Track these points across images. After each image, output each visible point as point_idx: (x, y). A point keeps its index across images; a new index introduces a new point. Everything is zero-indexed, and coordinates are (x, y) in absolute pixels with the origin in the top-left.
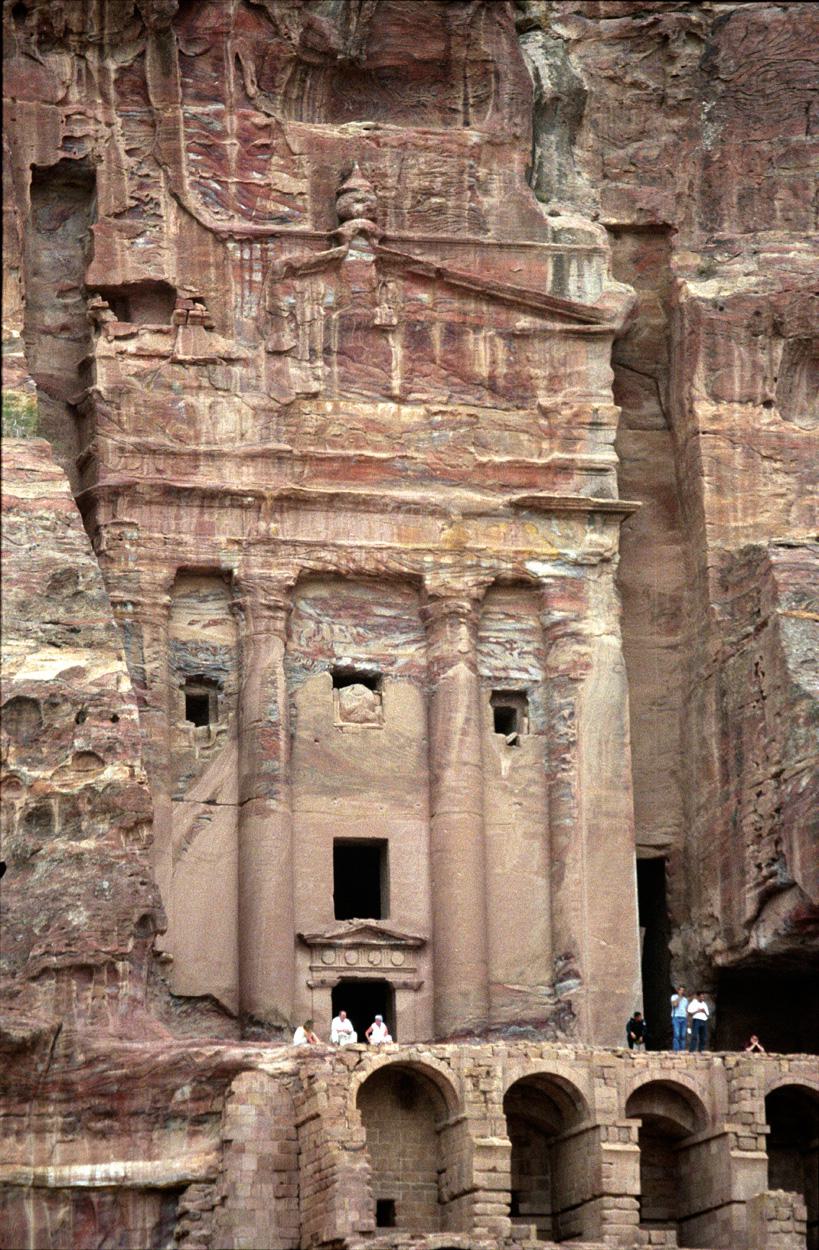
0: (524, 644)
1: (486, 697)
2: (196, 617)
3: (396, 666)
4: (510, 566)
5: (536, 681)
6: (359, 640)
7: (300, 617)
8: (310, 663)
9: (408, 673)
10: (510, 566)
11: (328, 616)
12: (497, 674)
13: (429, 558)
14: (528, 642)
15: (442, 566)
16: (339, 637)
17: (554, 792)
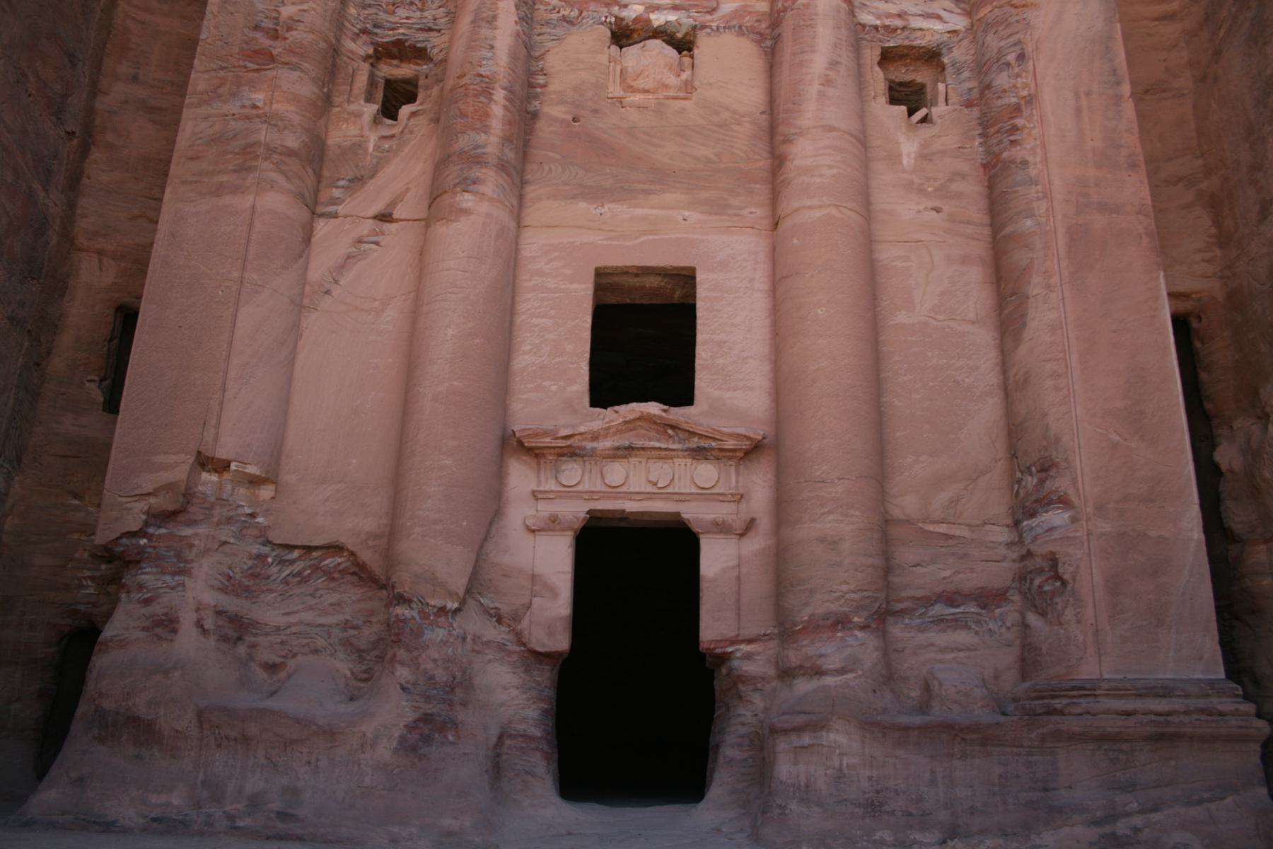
1: (871, 55)
3: (717, 15)
5: (954, 32)
8: (575, 13)
12: (887, 22)
17: (997, 177)
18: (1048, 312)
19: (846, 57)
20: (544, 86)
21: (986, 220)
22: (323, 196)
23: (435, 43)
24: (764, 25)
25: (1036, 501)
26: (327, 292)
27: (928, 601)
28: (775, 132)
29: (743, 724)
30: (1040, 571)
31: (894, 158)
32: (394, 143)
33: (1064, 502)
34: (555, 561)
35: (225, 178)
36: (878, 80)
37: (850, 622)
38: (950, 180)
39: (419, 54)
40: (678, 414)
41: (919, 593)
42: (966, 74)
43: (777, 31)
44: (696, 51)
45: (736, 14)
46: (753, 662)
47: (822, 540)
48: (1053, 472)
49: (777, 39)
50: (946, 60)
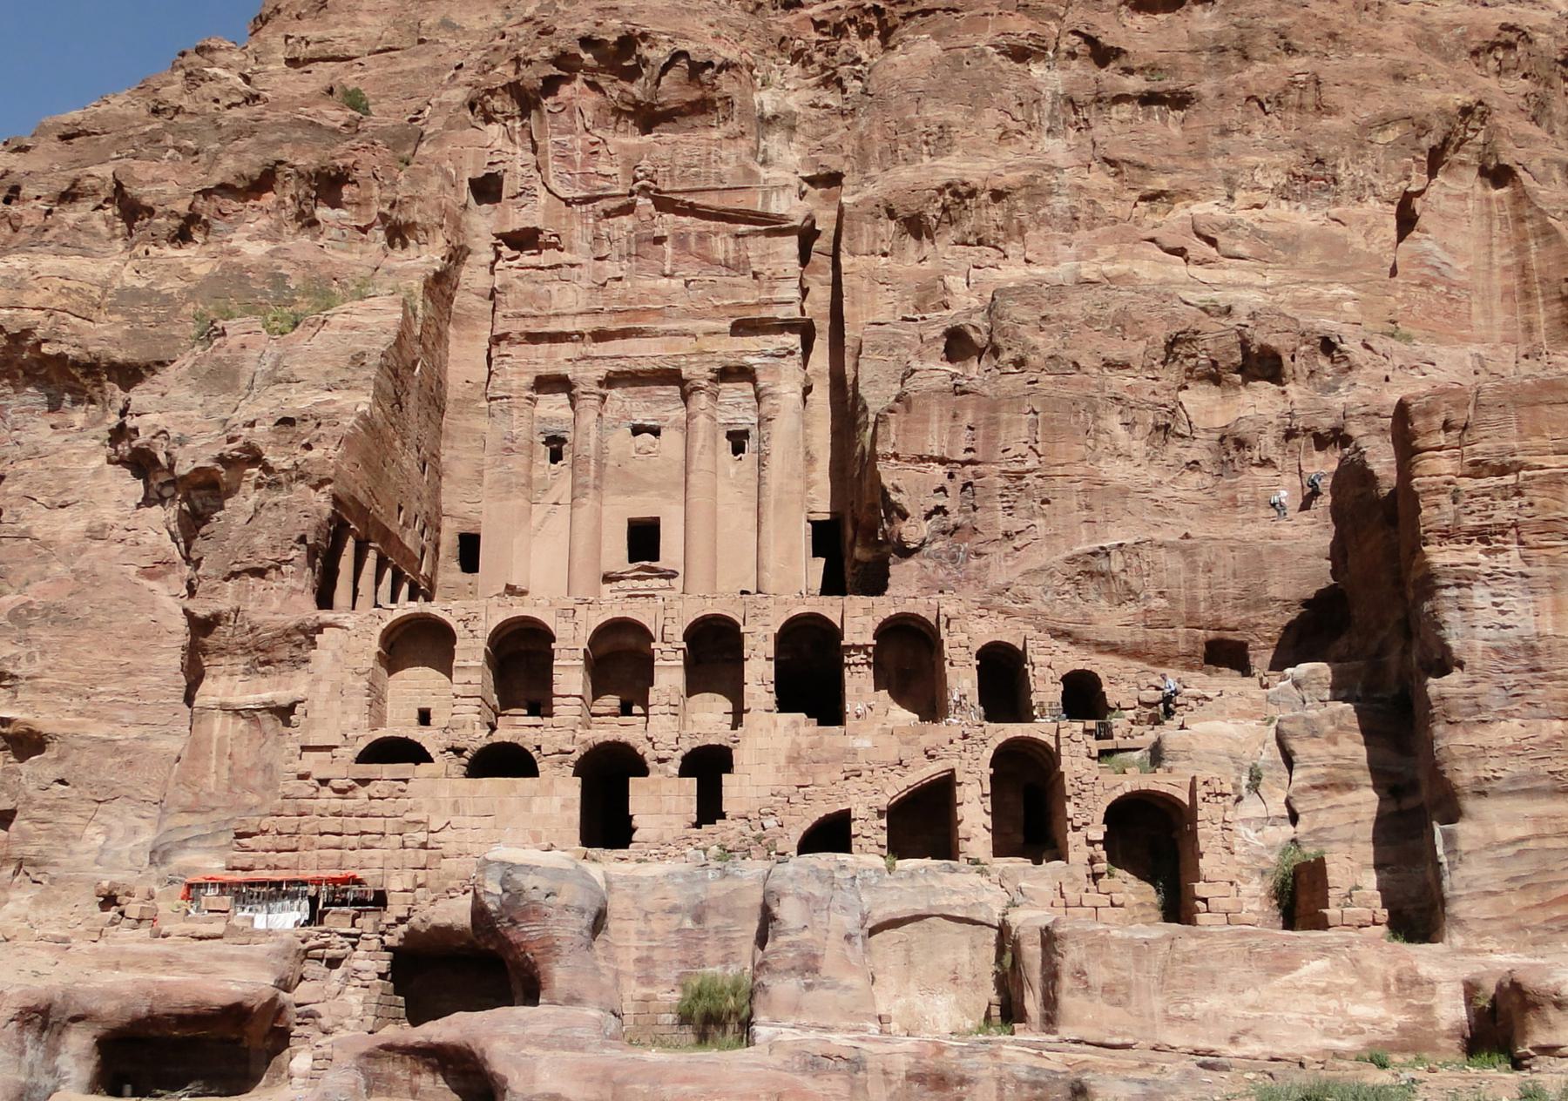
6: (647, 409)
9: (675, 426)
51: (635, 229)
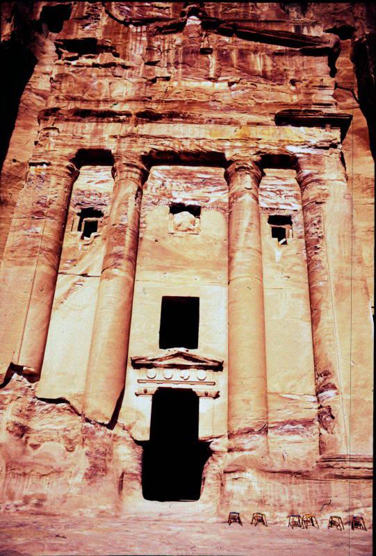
0: (288, 192)
1: (265, 219)
2: (92, 180)
3: (209, 203)
4: (276, 148)
6: (188, 189)
7: (153, 178)
8: (157, 200)
9: (217, 206)
10: (276, 148)
11: (170, 178)
12: (271, 206)
13: (228, 144)
14: (291, 191)
15: (235, 147)
16: (175, 187)
18: (329, 315)
19: (255, 221)
20: (145, 228)
21: (307, 281)
22: (61, 266)
23: (105, 210)
24: (226, 207)
25: (324, 386)
26: (62, 302)
27: (284, 423)
28: (230, 250)
29: (214, 470)
30: (325, 413)
31: (272, 259)
32: (88, 247)
33: (334, 387)
34: (144, 406)
35: (24, 259)
36: (267, 228)
37: (254, 431)
38: (294, 266)
39: (99, 214)
40: (191, 352)
41: (280, 420)
42: (300, 226)
43: (230, 210)
44: (201, 216)
45: (217, 202)
46: (218, 445)
47: (244, 400)
48: (329, 376)
49: (230, 213)
50: (292, 220)
51: (183, 43)
